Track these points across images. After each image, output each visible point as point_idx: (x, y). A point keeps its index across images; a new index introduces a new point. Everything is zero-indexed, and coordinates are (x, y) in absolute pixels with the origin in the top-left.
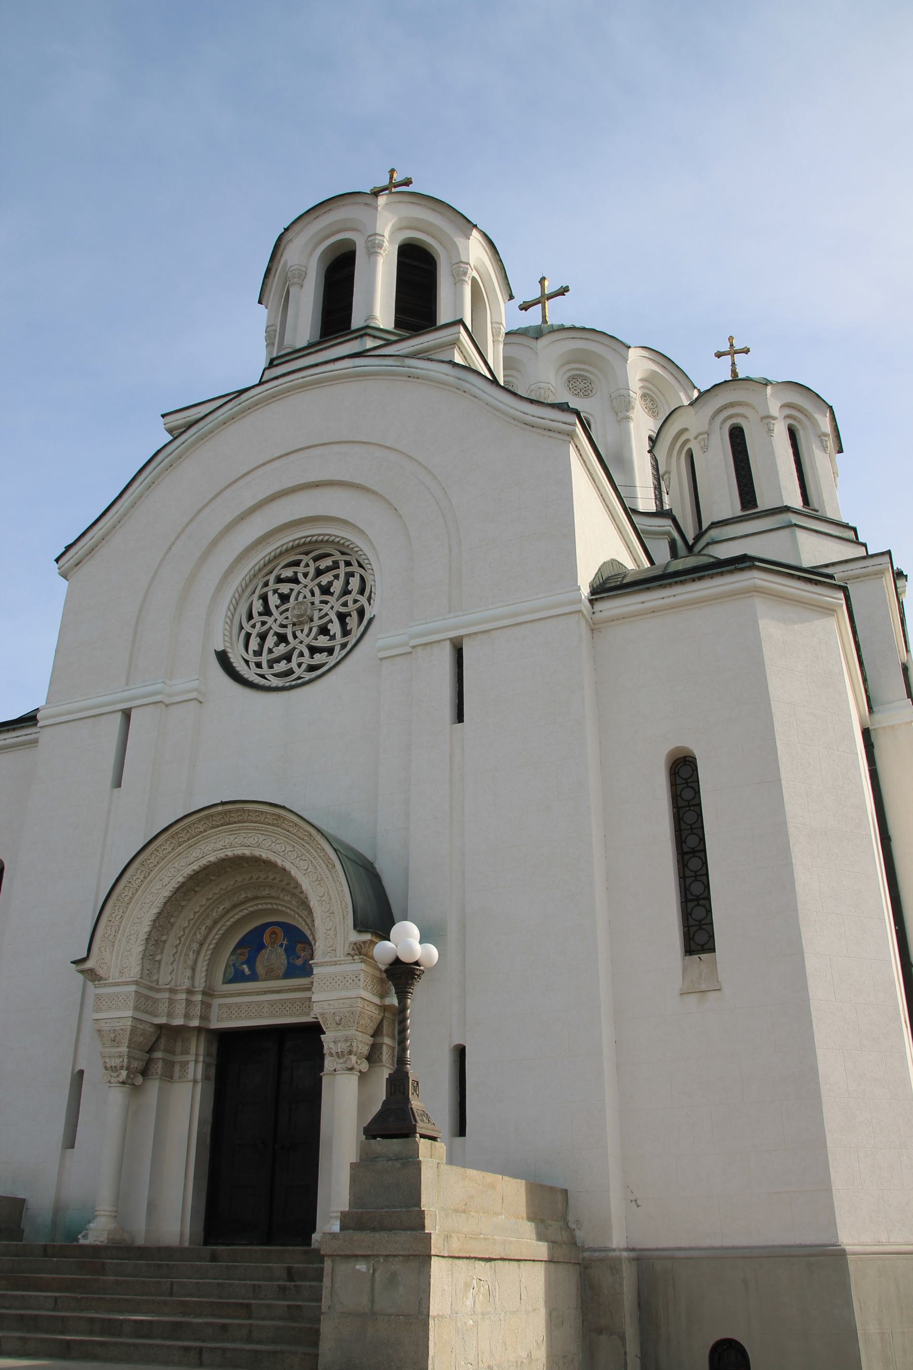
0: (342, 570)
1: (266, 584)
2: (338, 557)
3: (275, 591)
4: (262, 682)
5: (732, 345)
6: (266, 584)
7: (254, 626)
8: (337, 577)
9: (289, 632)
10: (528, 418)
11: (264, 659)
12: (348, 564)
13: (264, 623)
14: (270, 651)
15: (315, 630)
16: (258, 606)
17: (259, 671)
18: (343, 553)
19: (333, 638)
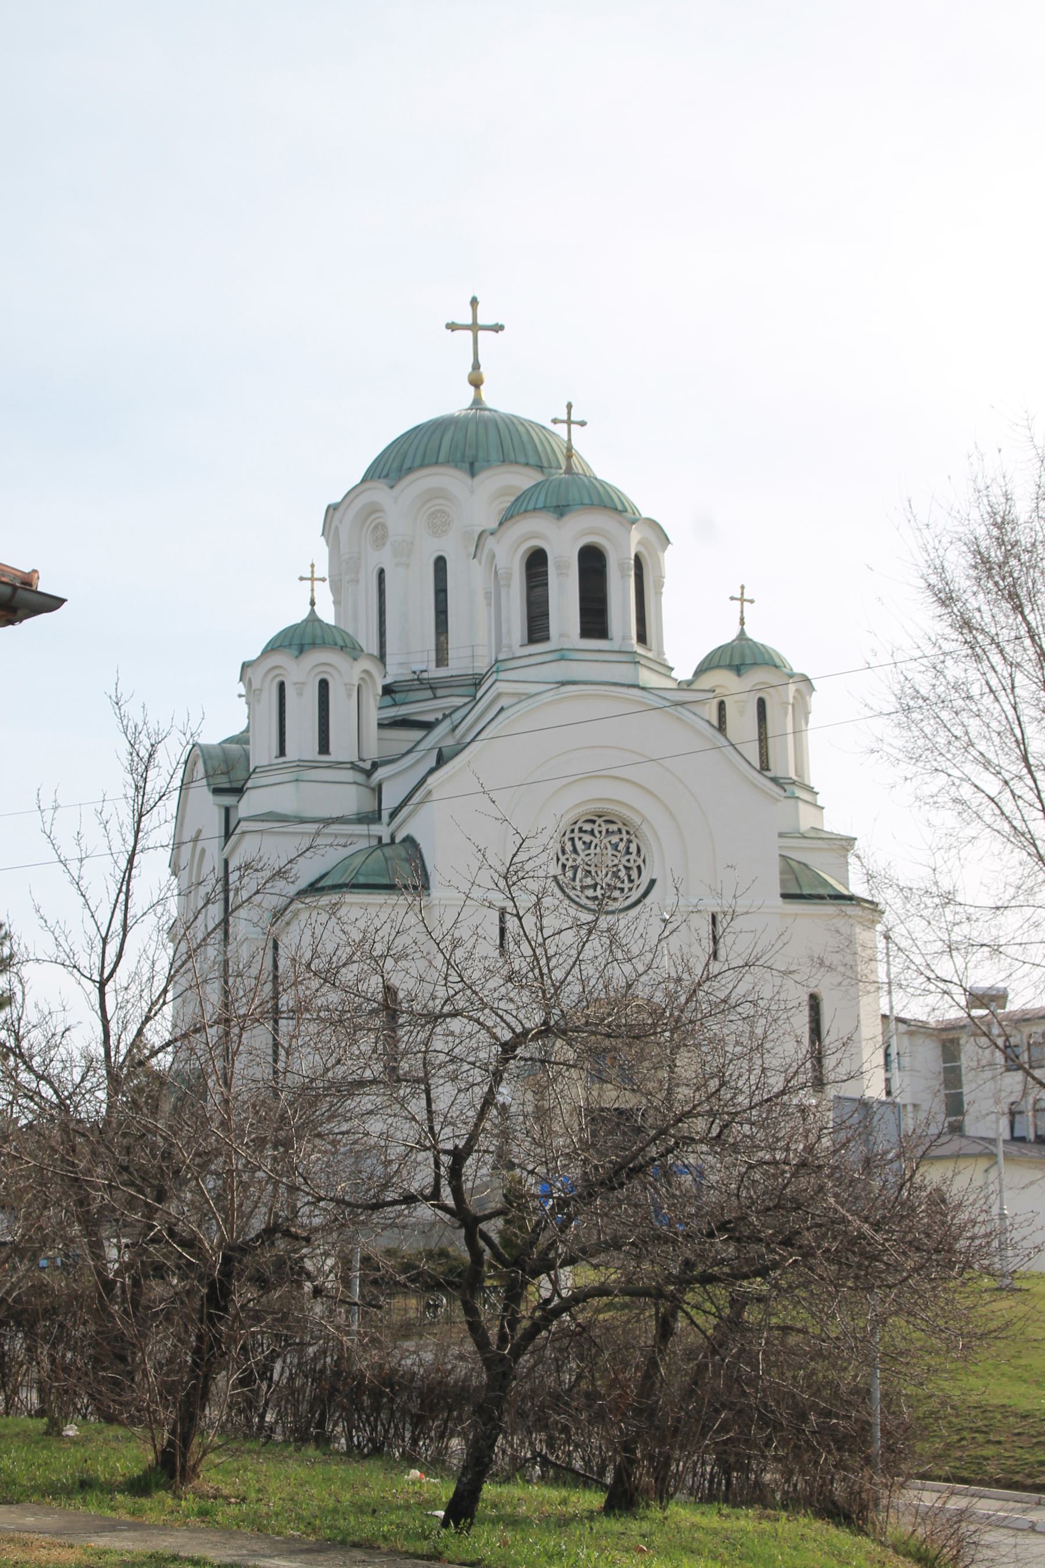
0: (625, 837)
1: (573, 831)
2: (620, 826)
3: (580, 839)
4: (577, 899)
5: (742, 594)
6: (573, 831)
7: (567, 859)
8: (621, 840)
9: (592, 869)
10: (756, 782)
11: (578, 883)
12: (628, 833)
13: (574, 860)
14: (581, 881)
15: (610, 874)
16: (569, 847)
17: (574, 892)
18: (624, 824)
19: (623, 882)
